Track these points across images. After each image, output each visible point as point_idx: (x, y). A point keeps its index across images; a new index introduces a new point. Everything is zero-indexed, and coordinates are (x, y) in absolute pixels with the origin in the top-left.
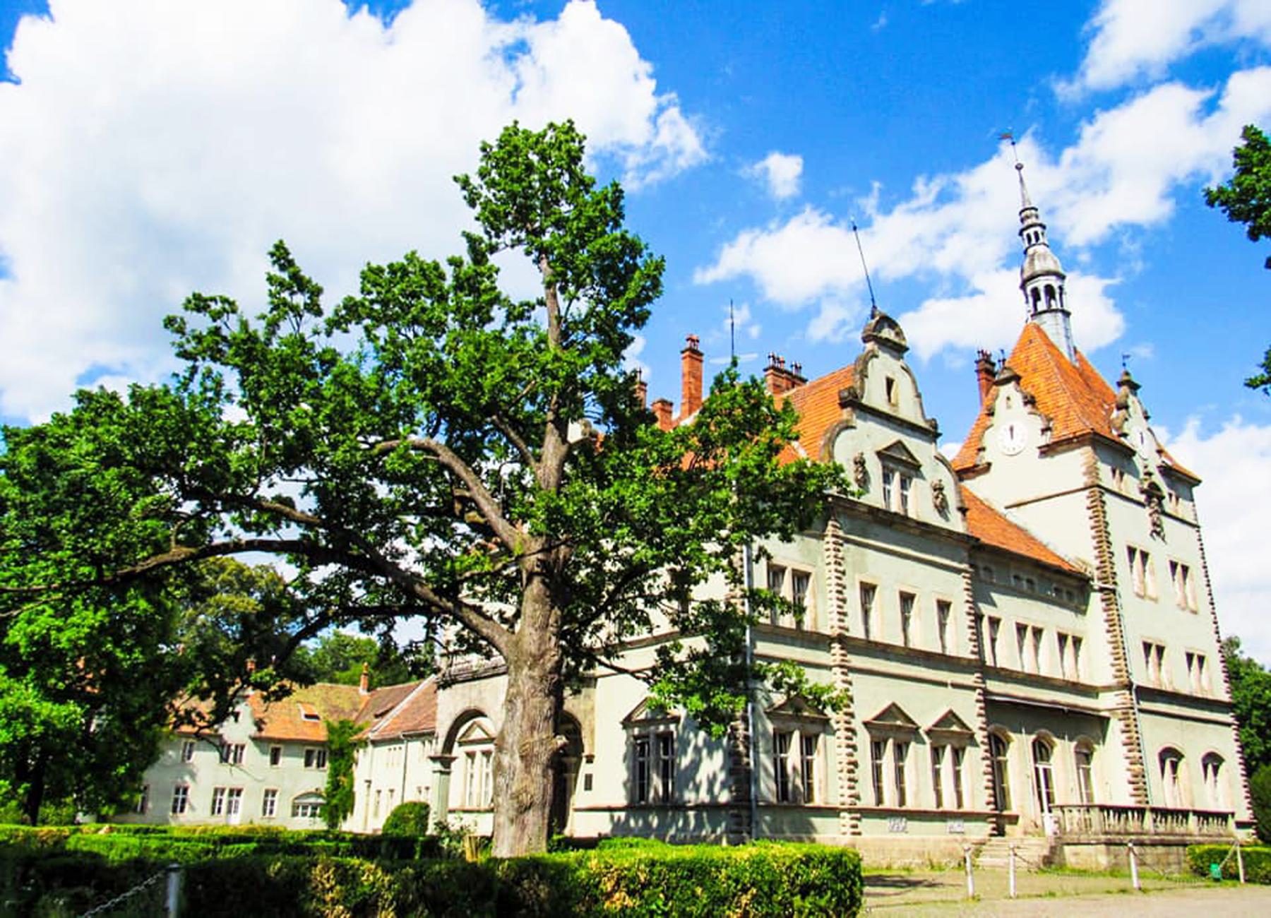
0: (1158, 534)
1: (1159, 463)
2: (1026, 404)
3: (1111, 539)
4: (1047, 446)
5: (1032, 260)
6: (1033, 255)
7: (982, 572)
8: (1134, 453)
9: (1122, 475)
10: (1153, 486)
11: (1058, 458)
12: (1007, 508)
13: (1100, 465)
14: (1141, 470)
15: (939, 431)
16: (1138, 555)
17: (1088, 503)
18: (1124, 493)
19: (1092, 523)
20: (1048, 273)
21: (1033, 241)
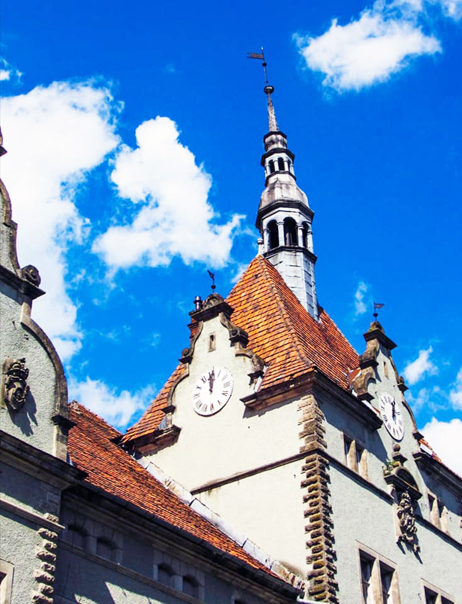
0: (410, 545)
1: (417, 450)
2: (233, 341)
3: (333, 532)
4: (254, 396)
5: (273, 188)
6: (275, 183)
7: (93, 546)
8: (378, 423)
9: (359, 451)
10: (404, 473)
11: (270, 415)
12: (193, 493)
13: (325, 424)
14: (390, 453)
15: (41, 287)
16: (376, 570)
17: (303, 478)
18: (361, 473)
19: (307, 507)
20: (289, 204)
21: (277, 168)
